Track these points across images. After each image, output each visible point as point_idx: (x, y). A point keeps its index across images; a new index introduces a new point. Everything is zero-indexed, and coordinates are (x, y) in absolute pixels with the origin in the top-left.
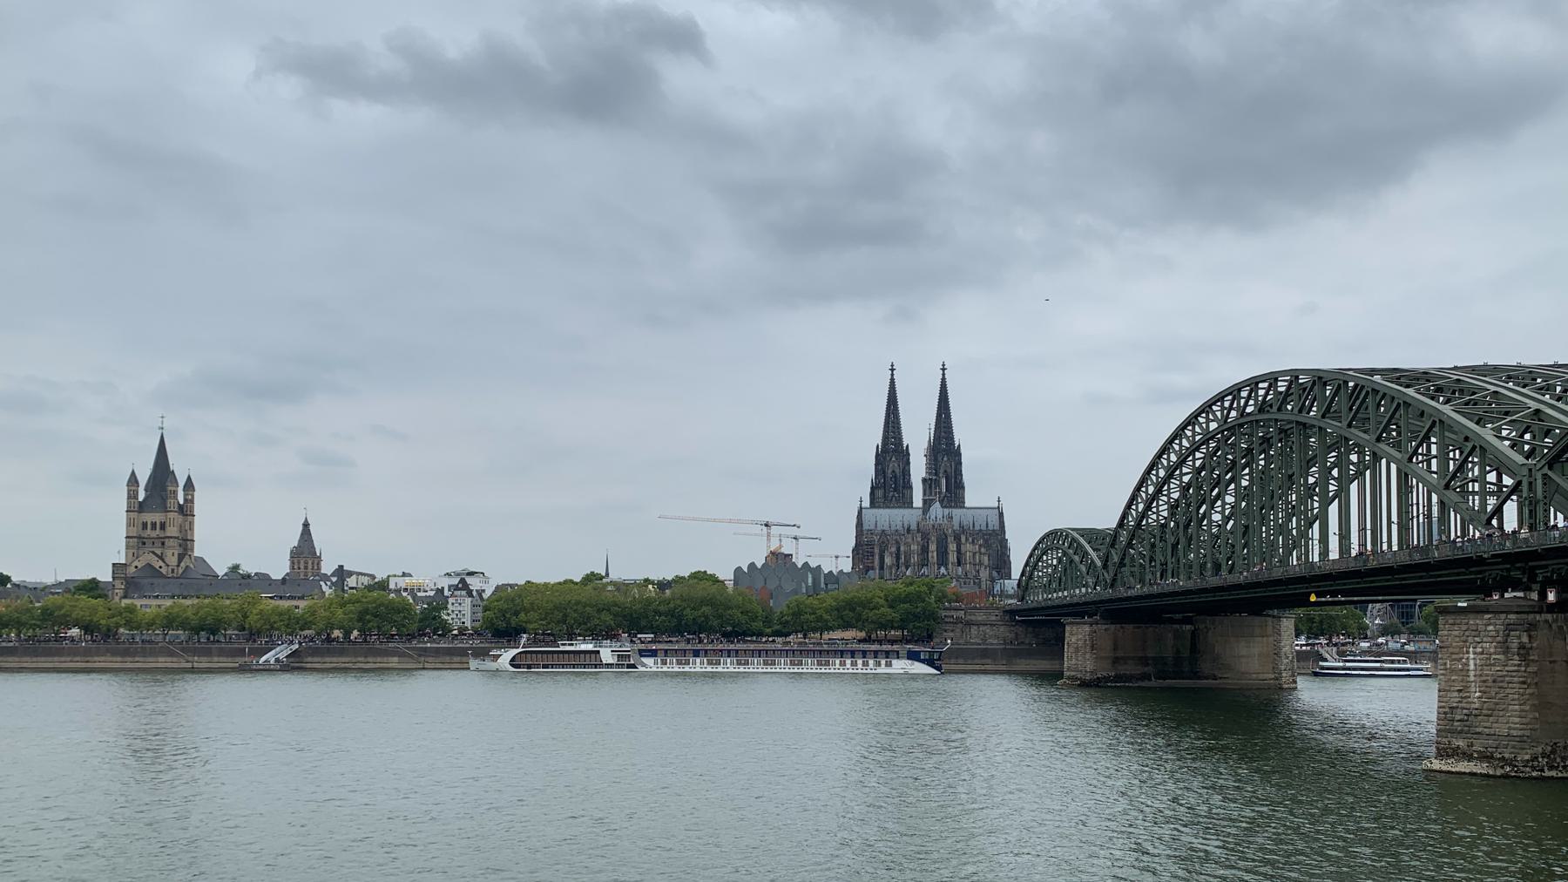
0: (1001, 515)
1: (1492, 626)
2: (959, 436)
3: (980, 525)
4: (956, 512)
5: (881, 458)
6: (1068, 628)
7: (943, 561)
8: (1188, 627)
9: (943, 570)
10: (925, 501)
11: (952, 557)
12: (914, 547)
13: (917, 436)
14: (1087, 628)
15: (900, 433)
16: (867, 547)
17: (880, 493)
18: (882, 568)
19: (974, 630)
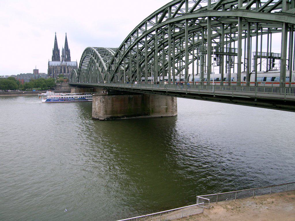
0: (77, 63)
1: (99, 98)
2: (70, 47)
3: (73, 65)
4: (68, 63)
5: (54, 52)
6: (71, 89)
7: (65, 72)
8: (93, 88)
9: (65, 74)
10: (62, 60)
11: (67, 71)
12: (59, 70)
13: (61, 46)
14: (75, 89)
15: (57, 45)
16: (51, 69)
17: (54, 58)
18: (53, 73)
19: (62, 87)
